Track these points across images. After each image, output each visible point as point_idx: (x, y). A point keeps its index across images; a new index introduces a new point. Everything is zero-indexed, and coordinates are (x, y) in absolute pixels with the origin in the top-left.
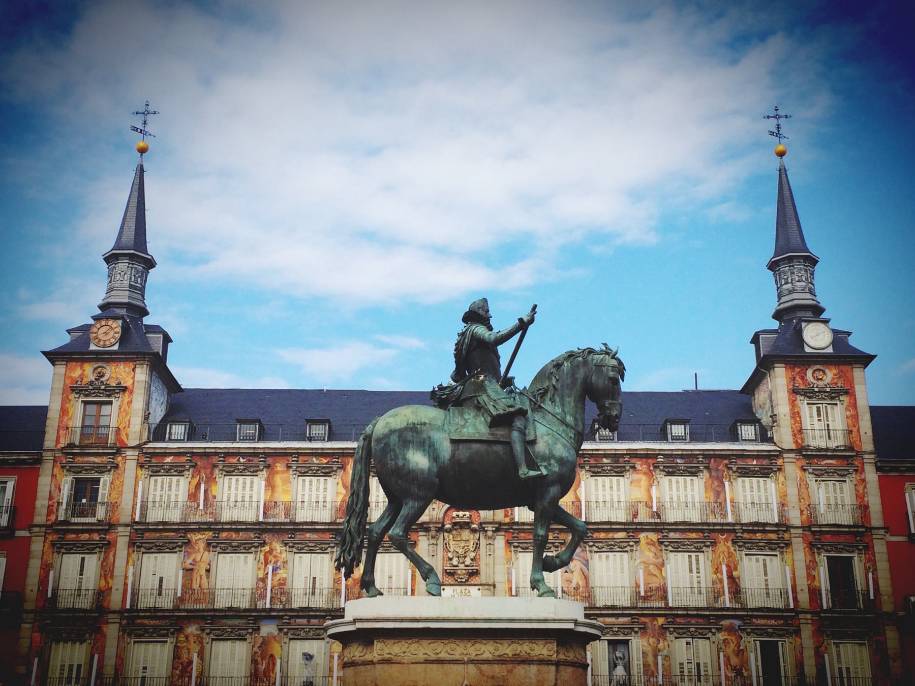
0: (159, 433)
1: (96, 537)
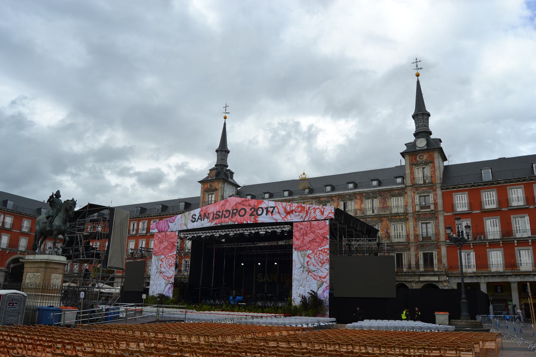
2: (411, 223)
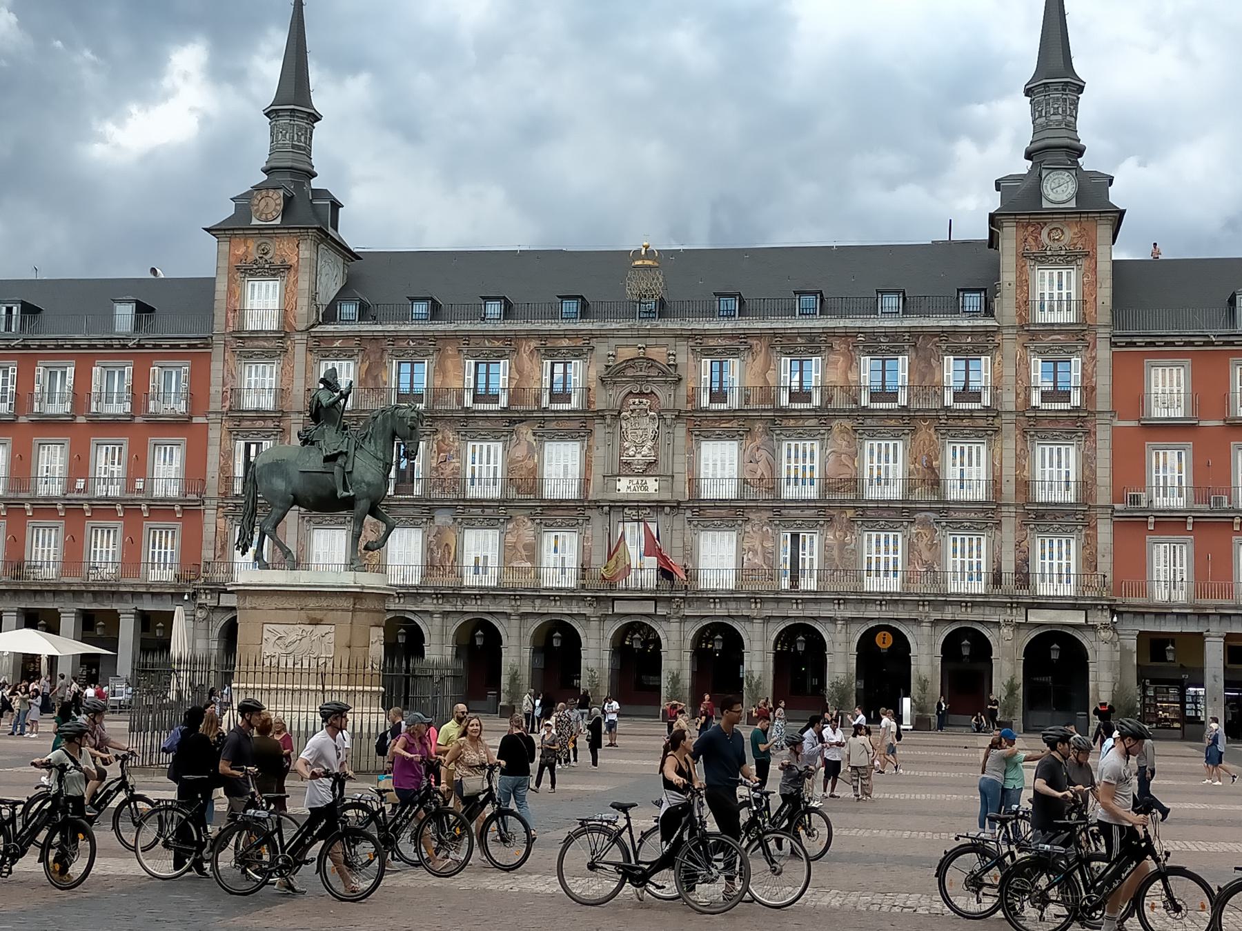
0: (330, 315)
1: (270, 424)
2: (1009, 445)
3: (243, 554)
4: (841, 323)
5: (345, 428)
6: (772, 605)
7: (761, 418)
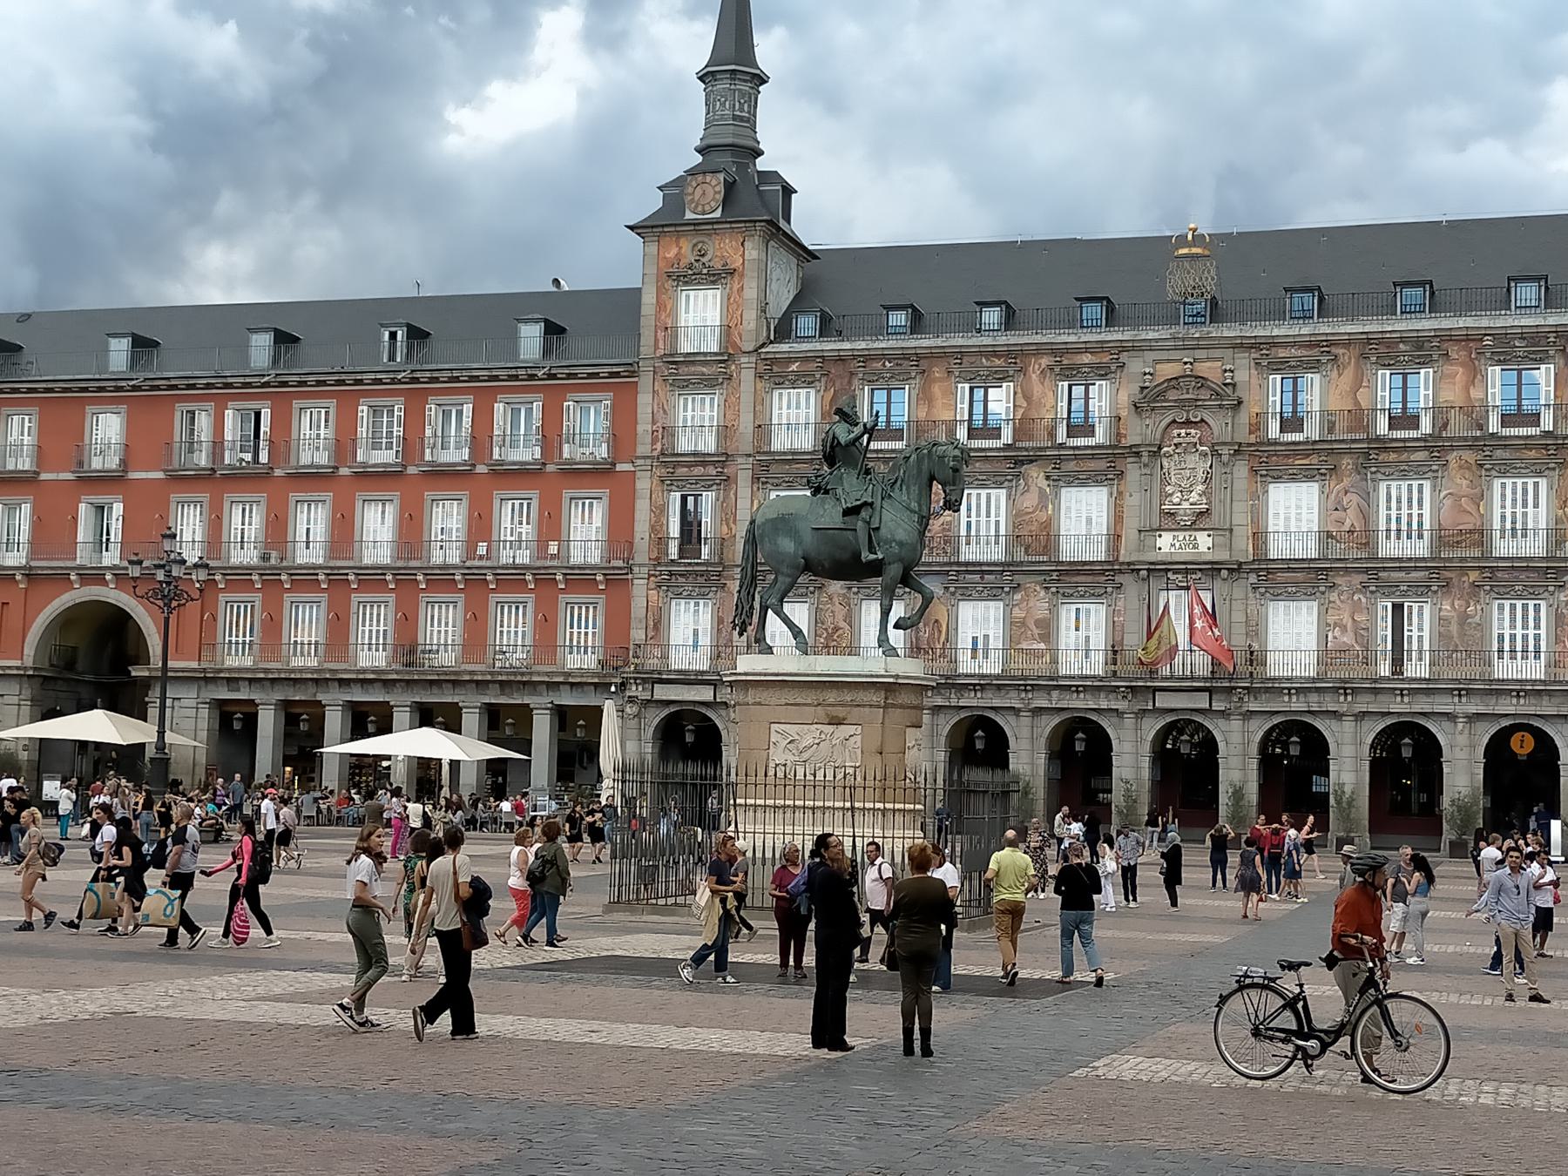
0: (783, 330)
1: (712, 471)
3: (741, 634)
4: (1462, 322)
5: (868, 472)
6: (1369, 698)
7: (1350, 451)
